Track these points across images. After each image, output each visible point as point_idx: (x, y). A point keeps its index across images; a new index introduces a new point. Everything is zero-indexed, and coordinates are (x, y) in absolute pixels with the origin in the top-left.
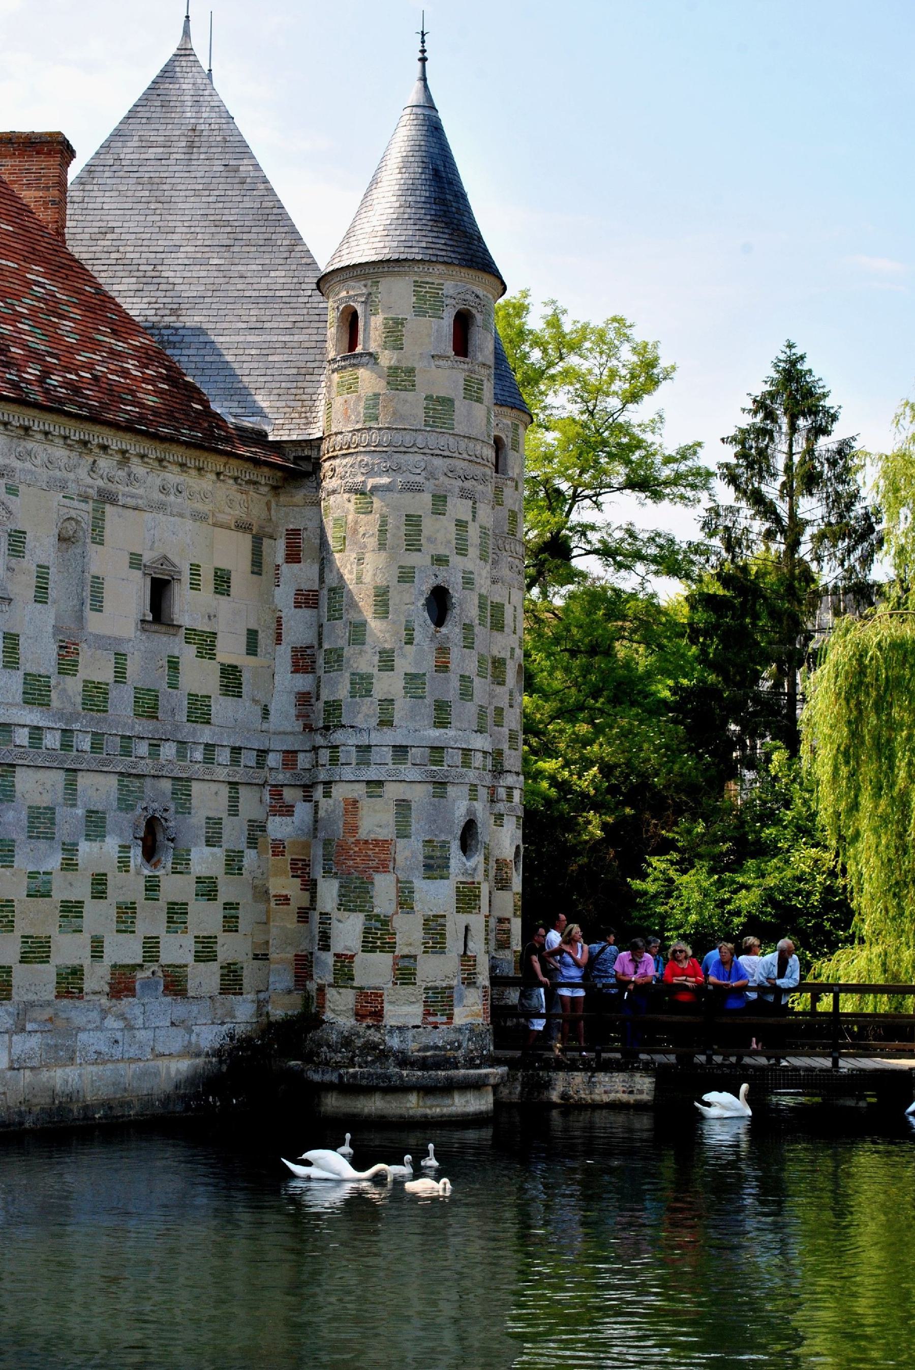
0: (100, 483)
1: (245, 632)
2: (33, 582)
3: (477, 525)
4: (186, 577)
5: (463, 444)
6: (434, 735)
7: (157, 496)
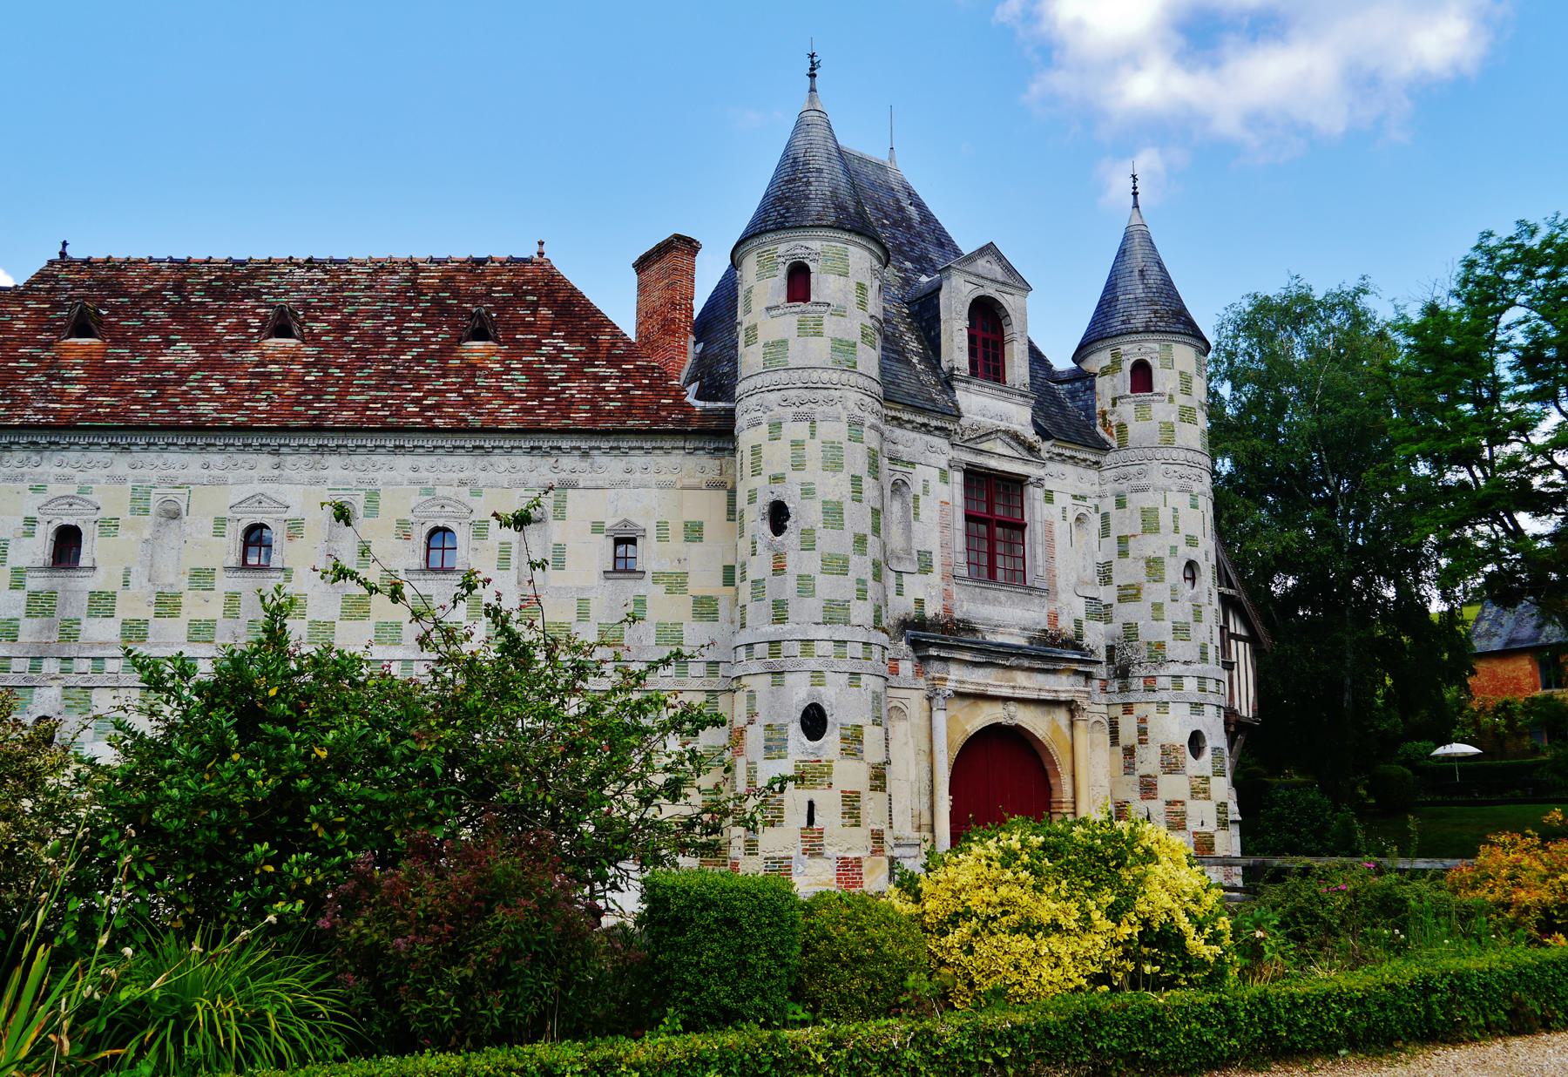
0: (563, 475)
1: (721, 569)
2: (497, 555)
3: (817, 441)
4: (652, 532)
5: (795, 375)
6: (772, 631)
7: (620, 476)
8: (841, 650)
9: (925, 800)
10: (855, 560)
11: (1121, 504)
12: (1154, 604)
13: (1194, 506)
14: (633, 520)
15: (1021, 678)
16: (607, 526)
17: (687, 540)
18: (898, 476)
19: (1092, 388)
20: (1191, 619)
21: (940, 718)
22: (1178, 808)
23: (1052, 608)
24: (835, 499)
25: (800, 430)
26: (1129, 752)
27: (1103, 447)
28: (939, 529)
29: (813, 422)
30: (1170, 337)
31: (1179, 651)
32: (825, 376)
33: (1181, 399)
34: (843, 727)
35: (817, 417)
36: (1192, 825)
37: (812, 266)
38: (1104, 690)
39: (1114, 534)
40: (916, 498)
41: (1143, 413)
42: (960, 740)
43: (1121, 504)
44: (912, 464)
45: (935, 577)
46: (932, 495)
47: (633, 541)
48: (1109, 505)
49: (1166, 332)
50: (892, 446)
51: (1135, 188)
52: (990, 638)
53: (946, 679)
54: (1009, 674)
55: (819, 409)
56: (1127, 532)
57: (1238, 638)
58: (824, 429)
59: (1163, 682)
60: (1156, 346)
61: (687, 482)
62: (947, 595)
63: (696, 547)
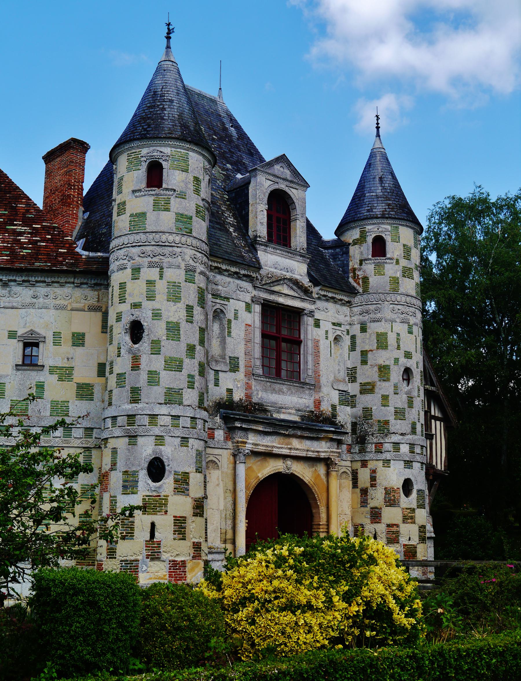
1: (96, 365)
4: (50, 339)
5: (151, 236)
6: (128, 408)
7: (29, 300)
8: (176, 422)
9: (229, 522)
10: (187, 361)
11: (363, 329)
12: (383, 396)
13: (410, 332)
14: (37, 330)
15: (296, 443)
16: (19, 334)
17: (74, 345)
18: (218, 306)
19: (347, 253)
20: (406, 406)
21: (241, 469)
22: (394, 529)
23: (317, 397)
24: (175, 320)
25: (153, 274)
26: (364, 492)
27: (352, 292)
28: (244, 343)
29: (162, 268)
30: (397, 222)
31: (398, 427)
32: (171, 238)
33: (404, 262)
34: (176, 473)
35: (165, 265)
36: (403, 540)
37: (164, 164)
38: (349, 451)
39: (358, 349)
40: (229, 321)
41: (379, 270)
42: (254, 483)
43: (363, 329)
44: (227, 299)
45: (241, 375)
46: (240, 320)
47: (37, 345)
48: (356, 330)
49: (395, 218)
50: (214, 287)
51: (378, 124)
52: (275, 415)
53: (245, 443)
54: (287, 440)
55: (166, 260)
56: (367, 348)
57: (436, 418)
58: (170, 273)
59: (388, 446)
60: (388, 227)
61: (75, 305)
62: (248, 387)
63: (79, 350)
